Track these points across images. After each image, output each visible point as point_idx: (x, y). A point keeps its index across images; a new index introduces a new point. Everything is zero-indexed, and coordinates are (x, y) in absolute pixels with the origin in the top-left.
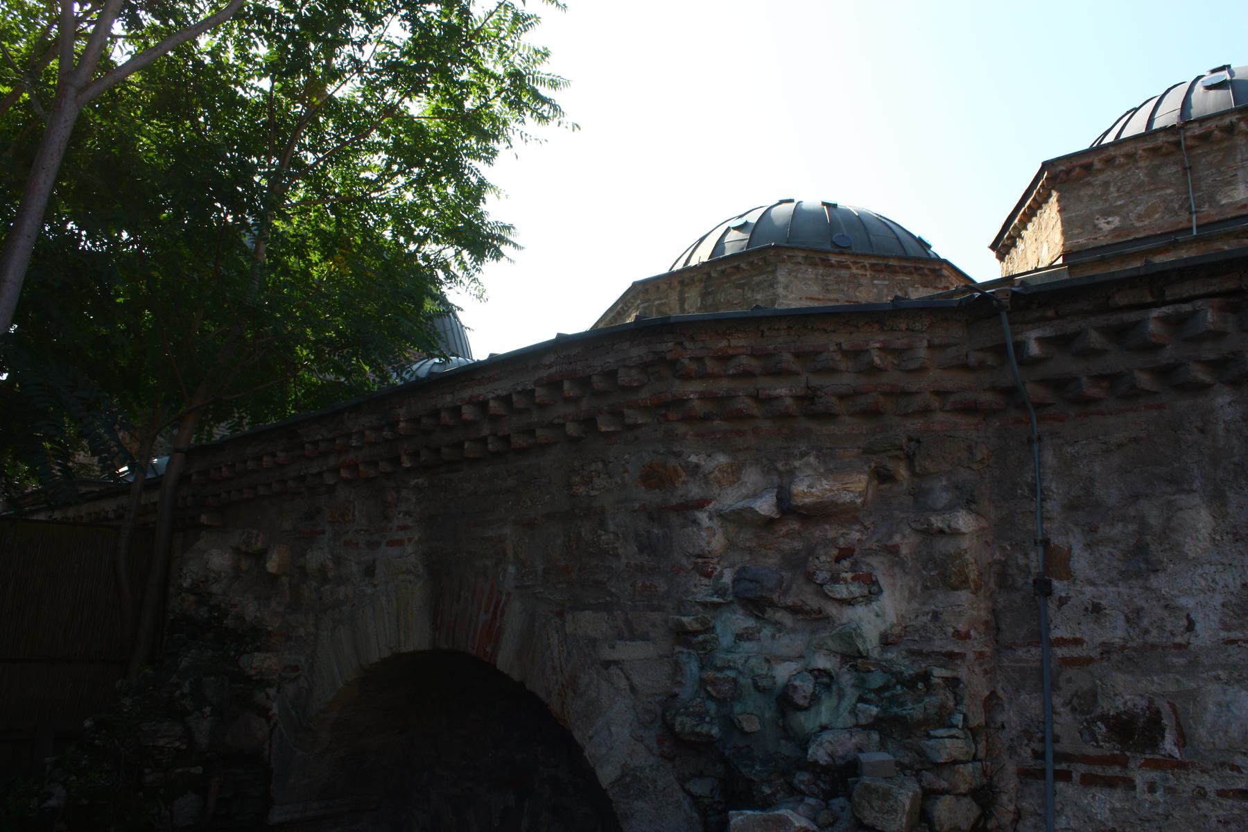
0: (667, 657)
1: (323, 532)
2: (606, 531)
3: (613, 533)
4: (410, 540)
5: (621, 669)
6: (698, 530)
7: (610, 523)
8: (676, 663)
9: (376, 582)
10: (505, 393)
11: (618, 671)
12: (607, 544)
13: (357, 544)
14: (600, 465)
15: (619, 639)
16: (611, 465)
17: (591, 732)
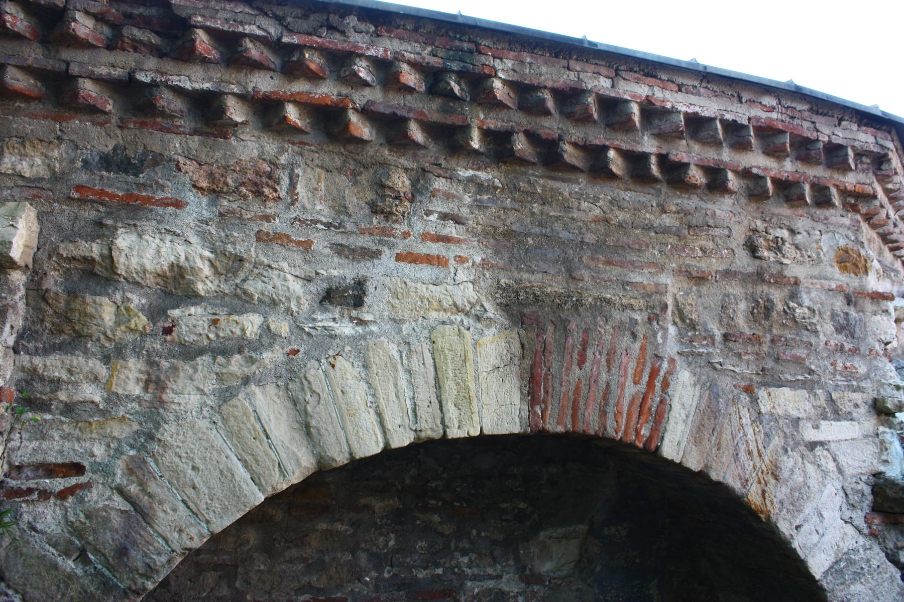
0: (871, 436)
1: (178, 204)
2: (800, 305)
3: (809, 308)
4: (461, 260)
5: (827, 450)
6: (888, 320)
7: (805, 296)
8: (882, 442)
9: (368, 317)
10: (706, 114)
11: (825, 452)
12: (804, 318)
13: (306, 246)
14: (785, 234)
15: (823, 419)
16: (799, 237)
17: (798, 521)
